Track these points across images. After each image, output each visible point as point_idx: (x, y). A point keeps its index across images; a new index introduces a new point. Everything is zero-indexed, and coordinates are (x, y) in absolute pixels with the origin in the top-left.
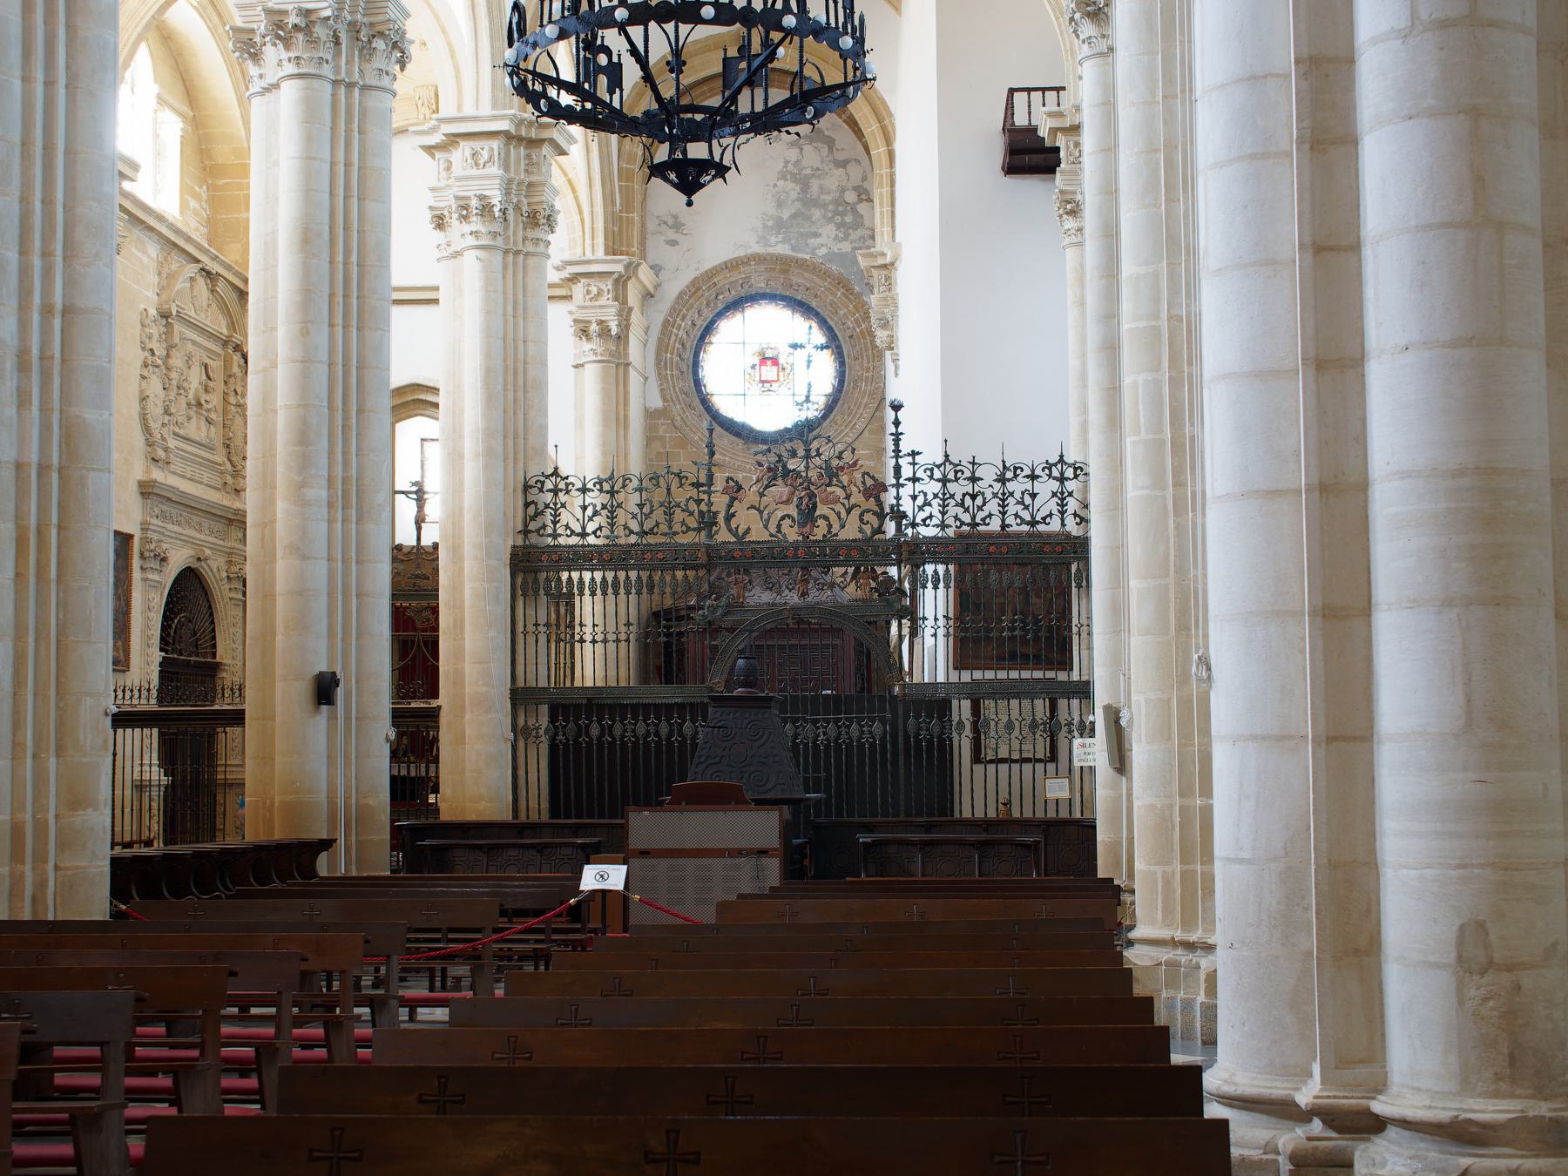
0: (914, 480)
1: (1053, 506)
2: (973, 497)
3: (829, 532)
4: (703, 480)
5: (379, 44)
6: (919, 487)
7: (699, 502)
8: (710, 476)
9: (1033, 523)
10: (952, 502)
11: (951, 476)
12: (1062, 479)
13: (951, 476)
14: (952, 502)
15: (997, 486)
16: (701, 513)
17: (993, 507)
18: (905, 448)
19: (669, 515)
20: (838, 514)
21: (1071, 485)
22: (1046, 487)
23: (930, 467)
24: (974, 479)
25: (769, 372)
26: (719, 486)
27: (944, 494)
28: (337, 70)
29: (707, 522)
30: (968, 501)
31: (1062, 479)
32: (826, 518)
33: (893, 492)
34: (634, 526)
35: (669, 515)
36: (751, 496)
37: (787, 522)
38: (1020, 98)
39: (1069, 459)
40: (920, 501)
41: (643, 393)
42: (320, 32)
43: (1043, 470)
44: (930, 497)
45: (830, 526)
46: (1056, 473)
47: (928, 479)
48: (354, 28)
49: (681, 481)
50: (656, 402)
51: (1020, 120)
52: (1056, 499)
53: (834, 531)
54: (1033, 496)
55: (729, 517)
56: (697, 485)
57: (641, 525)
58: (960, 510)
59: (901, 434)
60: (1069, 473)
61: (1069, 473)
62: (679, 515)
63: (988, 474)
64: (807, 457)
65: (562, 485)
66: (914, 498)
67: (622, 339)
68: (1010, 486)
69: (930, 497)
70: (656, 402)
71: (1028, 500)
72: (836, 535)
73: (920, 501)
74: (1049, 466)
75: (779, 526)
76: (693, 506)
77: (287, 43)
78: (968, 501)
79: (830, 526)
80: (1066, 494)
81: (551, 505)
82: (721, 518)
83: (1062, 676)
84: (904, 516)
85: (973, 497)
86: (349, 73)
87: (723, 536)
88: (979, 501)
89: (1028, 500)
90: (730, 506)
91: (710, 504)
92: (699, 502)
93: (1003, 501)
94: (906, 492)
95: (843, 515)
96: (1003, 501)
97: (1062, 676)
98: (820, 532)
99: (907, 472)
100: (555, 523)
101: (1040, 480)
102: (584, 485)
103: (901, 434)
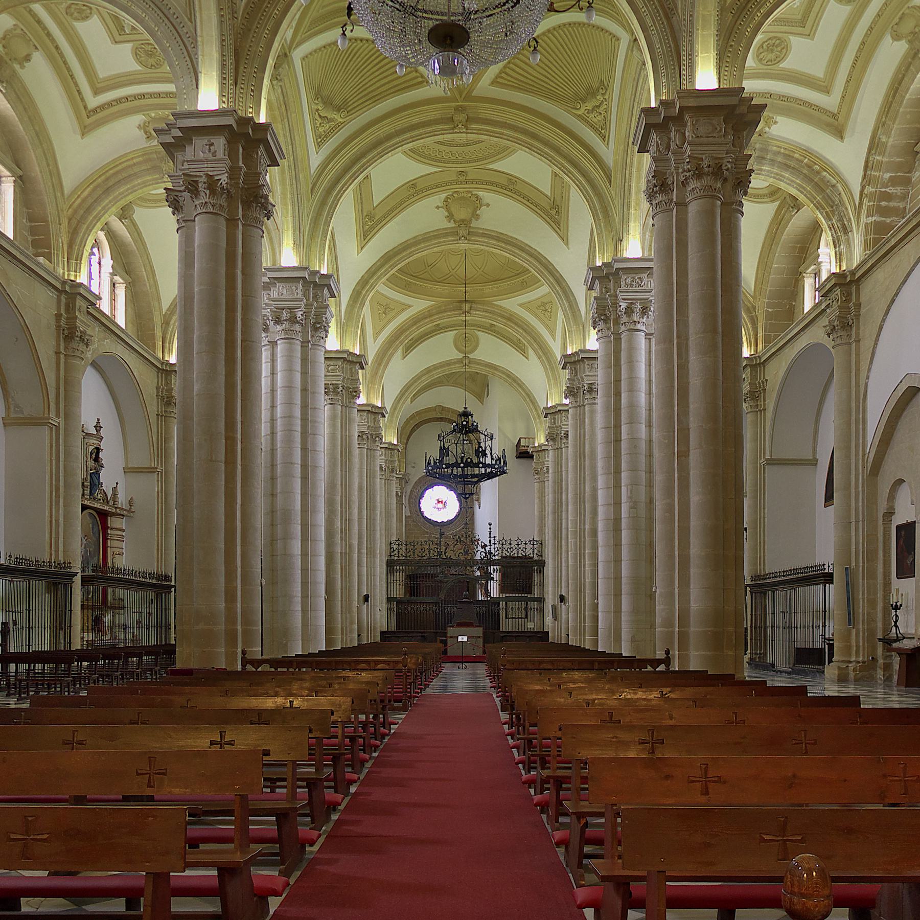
0: (495, 544)
2: (510, 549)
6: (496, 546)
7: (437, 549)
12: (533, 545)
15: (516, 546)
17: (515, 551)
18: (492, 536)
19: (429, 552)
21: (535, 546)
22: (529, 546)
25: (440, 505)
28: (368, 446)
29: (440, 554)
30: (509, 550)
31: (533, 545)
33: (489, 547)
34: (420, 554)
35: (429, 552)
36: (451, 548)
37: (461, 554)
40: (496, 549)
41: (406, 512)
54: (526, 549)
55: (445, 553)
56: (436, 544)
60: (535, 543)
61: (535, 543)
63: (514, 543)
66: (495, 549)
67: (401, 496)
71: (524, 550)
73: (496, 549)
76: (436, 549)
78: (509, 550)
82: (443, 553)
84: (492, 553)
85: (510, 549)
86: (371, 446)
88: (512, 550)
89: (524, 550)
92: (437, 549)
94: (493, 547)
99: (493, 542)
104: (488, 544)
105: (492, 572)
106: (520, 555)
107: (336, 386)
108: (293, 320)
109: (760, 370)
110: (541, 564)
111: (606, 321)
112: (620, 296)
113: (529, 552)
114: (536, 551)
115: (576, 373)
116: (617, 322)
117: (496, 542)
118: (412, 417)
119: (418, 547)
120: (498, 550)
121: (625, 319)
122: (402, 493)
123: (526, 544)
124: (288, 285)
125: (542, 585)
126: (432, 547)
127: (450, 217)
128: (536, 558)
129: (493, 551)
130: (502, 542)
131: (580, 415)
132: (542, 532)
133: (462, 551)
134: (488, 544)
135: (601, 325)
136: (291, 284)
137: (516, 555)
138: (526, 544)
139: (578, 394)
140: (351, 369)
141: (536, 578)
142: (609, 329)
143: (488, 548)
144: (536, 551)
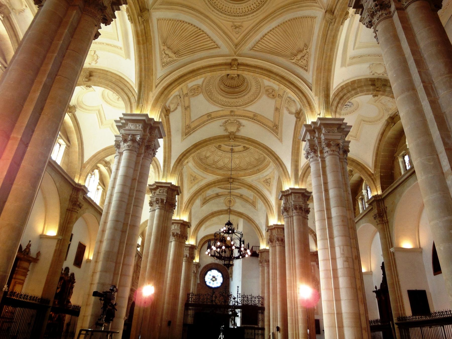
1: (258, 302)
9: (255, 304)
17: (250, 302)
18: (239, 293)
21: (260, 300)
22: (257, 300)
24: (248, 298)
25: (214, 279)
29: (212, 301)
31: (259, 299)
33: (237, 299)
35: (207, 300)
36: (218, 298)
38: (254, 248)
39: (260, 296)
41: (198, 281)
42: (178, 235)
48: (182, 236)
60: (260, 298)
61: (260, 298)
62: (208, 300)
63: (249, 297)
68: (252, 299)
74: (257, 297)
77: (174, 237)
83: (255, 326)
87: (214, 303)
94: (239, 299)
97: (255, 326)
104: (236, 297)
105: (238, 312)
107: (162, 201)
108: (134, 140)
109: (381, 203)
110: (263, 309)
111: (315, 152)
112: (323, 137)
113: (257, 302)
114: (260, 302)
115: (288, 200)
116: (322, 152)
118: (204, 238)
119: (202, 298)
121: (326, 149)
122: (197, 271)
123: (255, 298)
124: (134, 124)
125: (263, 320)
126: (208, 297)
127: (226, 130)
128: (260, 305)
129: (239, 301)
130: (243, 297)
131: (291, 221)
132: (263, 292)
133: (223, 300)
134: (236, 297)
135: (312, 154)
136: (136, 124)
138: (255, 298)
139: (289, 211)
140: (172, 193)
141: (260, 316)
142: (317, 156)
143: (236, 300)
144: (260, 302)
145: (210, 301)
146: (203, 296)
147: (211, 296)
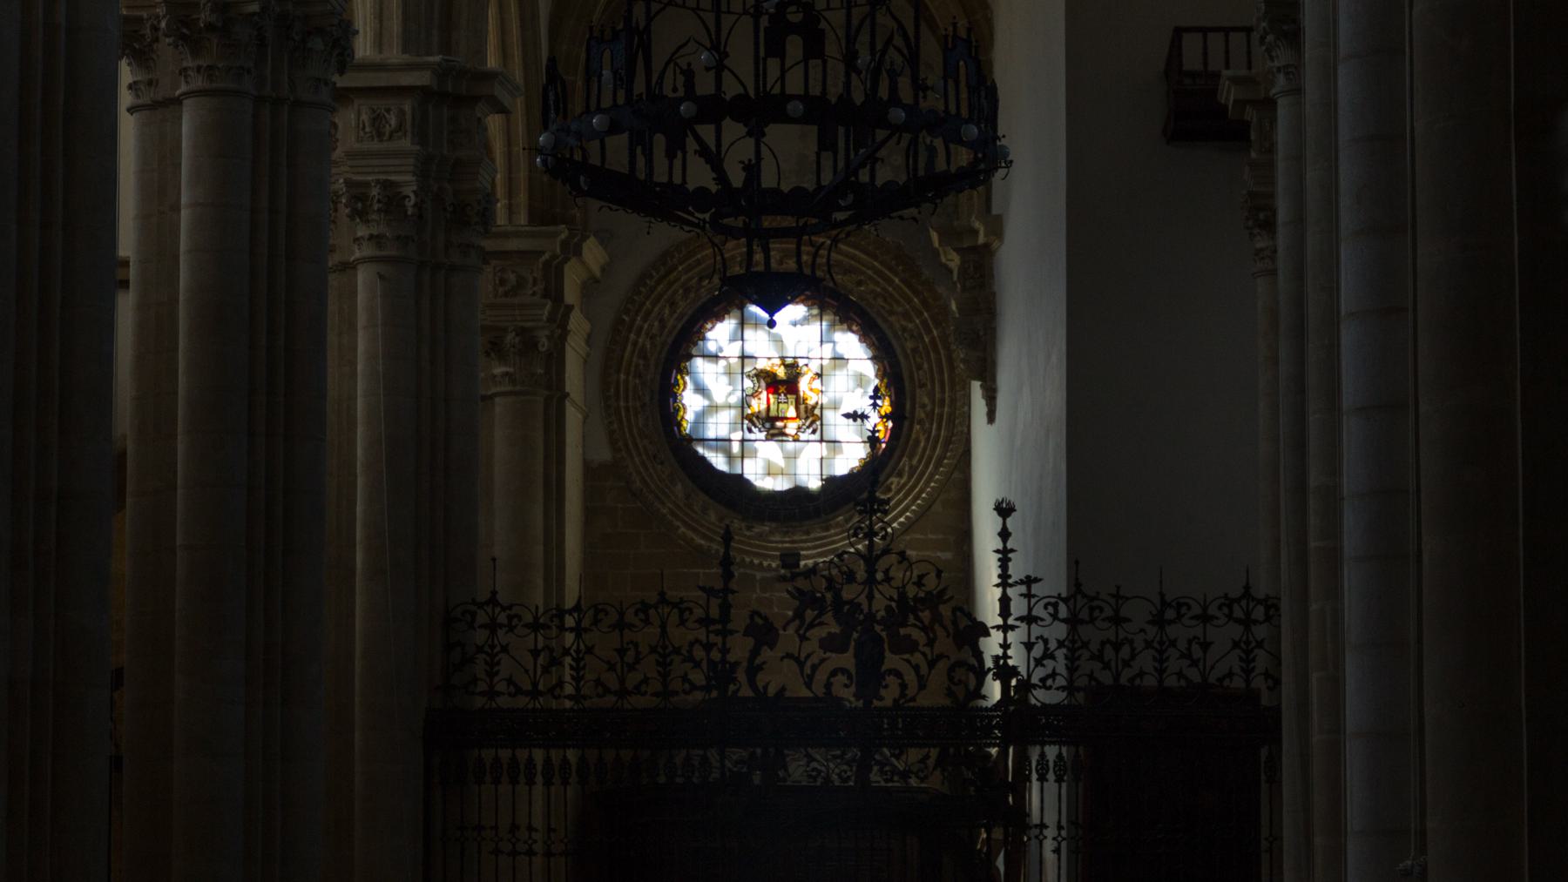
2: (1117, 647)
3: (903, 695)
4: (715, 612)
5: (317, 44)
6: (1036, 630)
8: (725, 608)
10: (1086, 654)
11: (1084, 615)
12: (1247, 622)
13: (1084, 615)
14: (1086, 654)
15: (1152, 631)
16: (711, 662)
17: (1146, 661)
20: (916, 668)
21: (1260, 632)
23: (1053, 600)
24: (1117, 620)
26: (739, 619)
27: (1073, 642)
29: (722, 674)
30: (1109, 653)
31: (1247, 622)
32: (898, 674)
33: (997, 637)
34: (612, 681)
36: (788, 638)
37: (841, 679)
38: (1191, 44)
40: (1038, 651)
43: (1220, 608)
44: (1053, 645)
45: (903, 686)
46: (1238, 612)
47: (1049, 619)
49: (681, 615)
50: (604, 454)
51: (1191, 59)
52: (1238, 651)
53: (910, 692)
54: (1206, 646)
55: (753, 671)
56: (705, 621)
57: (622, 681)
58: (1097, 665)
59: (1012, 551)
60: (1259, 613)
61: (1259, 613)
64: (871, 581)
65: (502, 618)
68: (1172, 631)
69: (1053, 645)
70: (604, 454)
71: (1197, 652)
72: (913, 699)
74: (1229, 602)
75: (828, 685)
76: (699, 653)
78: (1109, 653)
79: (903, 686)
80: (1253, 644)
81: (487, 649)
82: (741, 676)
85: (1117, 647)
88: (1125, 651)
89: (1197, 652)
90: (755, 653)
91: (725, 651)
92: (708, 647)
93: (1161, 652)
95: (924, 670)
96: (1161, 652)
98: (889, 694)
100: (491, 675)
101: (1215, 622)
102: (536, 618)
103: (1012, 551)
106: (1171, 681)
117: (1039, 611)
120: (1048, 655)
123: (1205, 618)
129: (1016, 658)
133: (847, 660)
137: (1150, 681)
138: (1205, 618)
145: (698, 677)
146: (621, 625)
147: (705, 621)
